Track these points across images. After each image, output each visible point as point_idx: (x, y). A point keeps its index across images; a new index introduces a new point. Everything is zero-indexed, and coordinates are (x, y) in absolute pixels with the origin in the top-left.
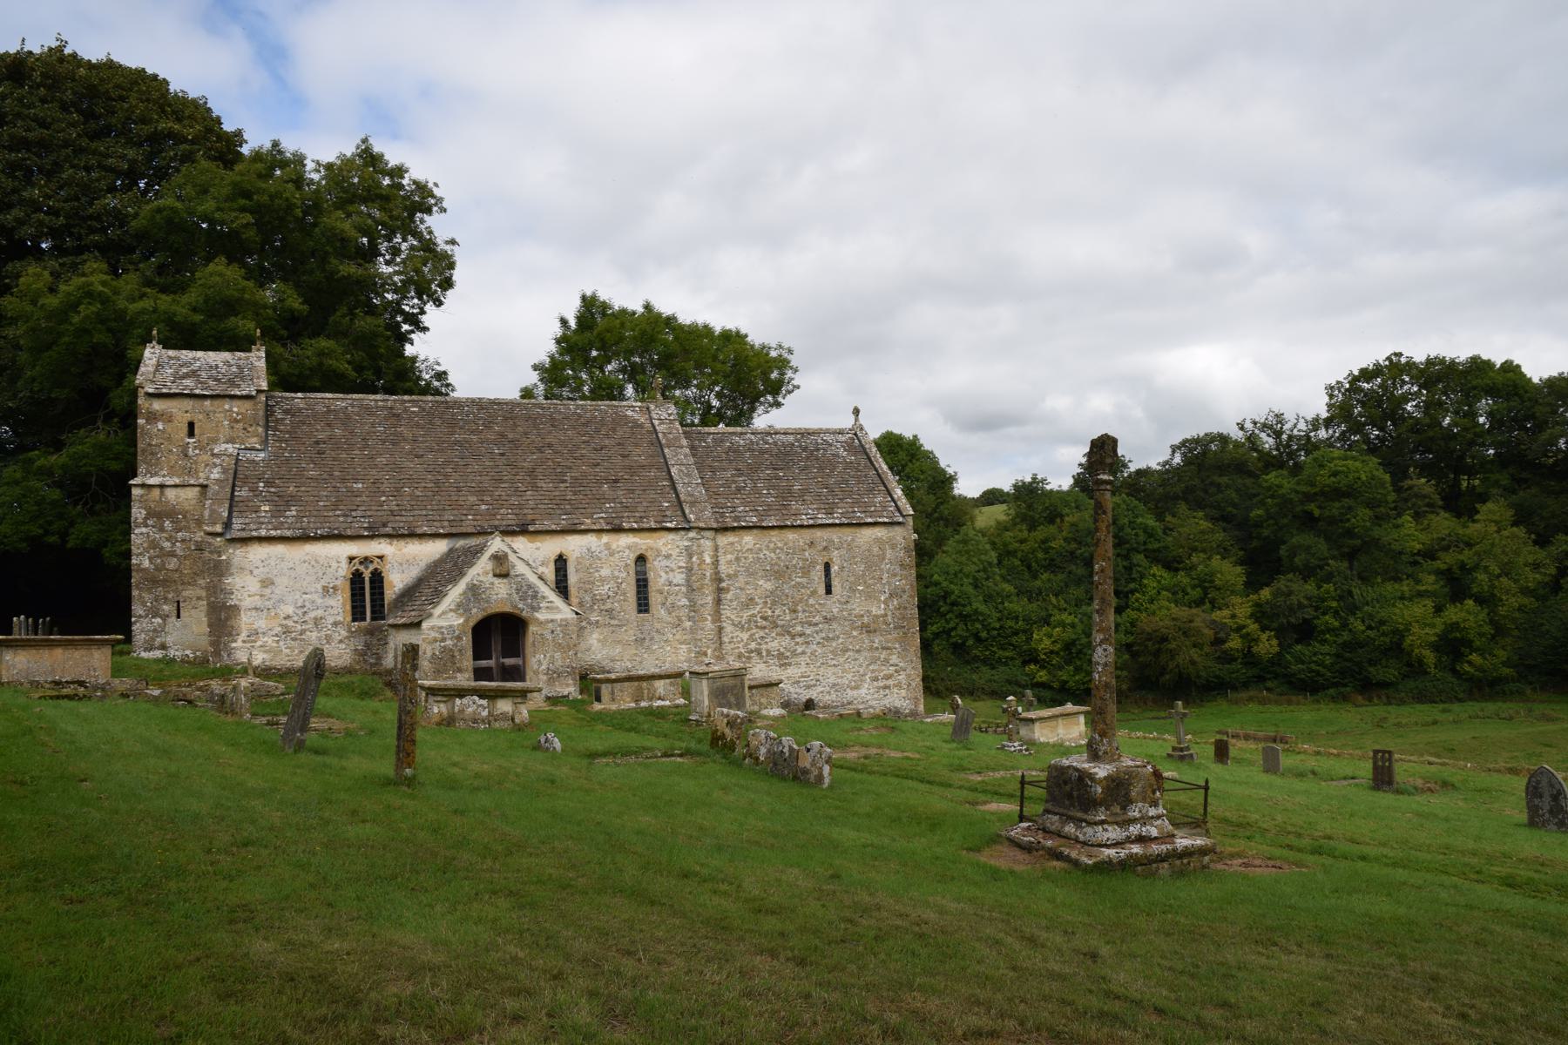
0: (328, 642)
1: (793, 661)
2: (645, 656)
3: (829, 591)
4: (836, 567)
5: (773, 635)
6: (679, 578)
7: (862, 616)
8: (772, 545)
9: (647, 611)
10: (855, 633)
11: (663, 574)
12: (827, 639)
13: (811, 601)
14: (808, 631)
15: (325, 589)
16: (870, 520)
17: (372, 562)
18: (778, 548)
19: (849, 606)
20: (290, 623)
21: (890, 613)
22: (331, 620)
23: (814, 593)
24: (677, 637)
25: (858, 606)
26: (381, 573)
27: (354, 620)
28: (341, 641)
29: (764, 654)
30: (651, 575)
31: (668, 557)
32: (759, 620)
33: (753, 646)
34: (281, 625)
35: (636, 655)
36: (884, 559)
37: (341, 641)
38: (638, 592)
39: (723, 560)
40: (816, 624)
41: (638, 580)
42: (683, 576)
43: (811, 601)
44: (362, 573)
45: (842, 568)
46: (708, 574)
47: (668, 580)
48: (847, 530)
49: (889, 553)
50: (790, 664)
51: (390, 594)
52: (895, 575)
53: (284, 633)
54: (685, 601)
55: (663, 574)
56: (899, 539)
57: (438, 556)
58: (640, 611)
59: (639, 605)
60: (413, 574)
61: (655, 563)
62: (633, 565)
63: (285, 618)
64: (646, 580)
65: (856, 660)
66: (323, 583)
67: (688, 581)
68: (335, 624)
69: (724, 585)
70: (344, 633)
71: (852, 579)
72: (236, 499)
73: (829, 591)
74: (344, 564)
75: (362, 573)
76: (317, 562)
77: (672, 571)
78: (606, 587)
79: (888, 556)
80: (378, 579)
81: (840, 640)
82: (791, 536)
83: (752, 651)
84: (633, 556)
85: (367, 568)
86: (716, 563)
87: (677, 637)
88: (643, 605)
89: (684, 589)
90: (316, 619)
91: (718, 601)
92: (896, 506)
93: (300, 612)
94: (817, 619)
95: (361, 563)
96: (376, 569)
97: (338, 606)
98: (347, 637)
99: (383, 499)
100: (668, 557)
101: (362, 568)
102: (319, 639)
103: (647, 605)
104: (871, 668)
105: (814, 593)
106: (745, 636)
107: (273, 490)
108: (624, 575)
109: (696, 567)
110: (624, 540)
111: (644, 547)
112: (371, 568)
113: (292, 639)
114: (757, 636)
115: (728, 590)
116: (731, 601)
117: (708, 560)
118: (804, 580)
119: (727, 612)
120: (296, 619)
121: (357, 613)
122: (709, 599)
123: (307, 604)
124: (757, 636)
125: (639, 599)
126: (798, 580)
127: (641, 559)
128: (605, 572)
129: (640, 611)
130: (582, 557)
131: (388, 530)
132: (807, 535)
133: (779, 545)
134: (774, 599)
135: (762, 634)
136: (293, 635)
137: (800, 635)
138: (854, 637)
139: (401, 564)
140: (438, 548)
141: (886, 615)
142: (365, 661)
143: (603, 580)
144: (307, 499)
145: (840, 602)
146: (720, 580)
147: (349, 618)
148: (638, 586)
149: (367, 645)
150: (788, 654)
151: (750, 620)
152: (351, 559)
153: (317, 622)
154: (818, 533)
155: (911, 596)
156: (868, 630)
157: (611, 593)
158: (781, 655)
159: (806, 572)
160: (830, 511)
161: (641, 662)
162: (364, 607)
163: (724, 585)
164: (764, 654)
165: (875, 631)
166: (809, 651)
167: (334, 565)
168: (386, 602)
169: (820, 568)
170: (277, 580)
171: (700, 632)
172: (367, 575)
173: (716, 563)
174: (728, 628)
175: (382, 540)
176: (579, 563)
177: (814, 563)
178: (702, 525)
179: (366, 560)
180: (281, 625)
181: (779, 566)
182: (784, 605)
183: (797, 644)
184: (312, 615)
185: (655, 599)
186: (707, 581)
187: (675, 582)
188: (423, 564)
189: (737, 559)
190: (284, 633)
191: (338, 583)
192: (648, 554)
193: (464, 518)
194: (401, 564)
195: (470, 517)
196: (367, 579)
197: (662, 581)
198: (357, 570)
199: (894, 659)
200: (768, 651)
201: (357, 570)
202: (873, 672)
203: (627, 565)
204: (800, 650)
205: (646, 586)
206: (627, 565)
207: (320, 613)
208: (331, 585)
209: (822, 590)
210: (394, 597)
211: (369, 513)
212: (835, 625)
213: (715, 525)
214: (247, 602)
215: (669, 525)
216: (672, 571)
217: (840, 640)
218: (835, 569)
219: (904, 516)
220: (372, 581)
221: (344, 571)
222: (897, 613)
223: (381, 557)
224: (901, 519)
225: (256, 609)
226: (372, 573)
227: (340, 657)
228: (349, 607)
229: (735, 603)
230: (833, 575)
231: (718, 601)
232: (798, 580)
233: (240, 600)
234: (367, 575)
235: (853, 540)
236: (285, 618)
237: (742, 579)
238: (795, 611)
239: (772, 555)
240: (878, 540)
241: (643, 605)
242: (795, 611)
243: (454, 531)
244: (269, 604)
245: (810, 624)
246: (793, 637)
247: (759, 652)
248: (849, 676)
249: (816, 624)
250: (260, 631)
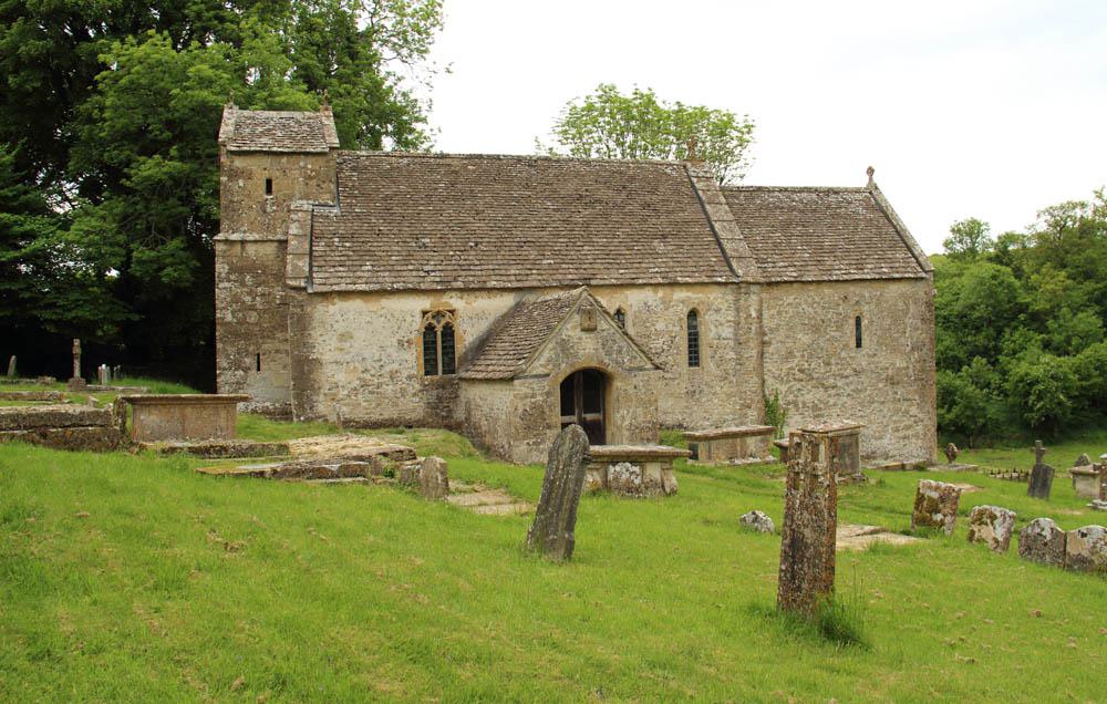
0: (403, 396)
1: (825, 412)
2: (696, 408)
3: (859, 345)
4: (866, 321)
5: (809, 387)
6: (727, 332)
7: (887, 369)
8: (810, 300)
9: (697, 364)
10: (881, 385)
11: (713, 328)
12: (857, 391)
13: (843, 354)
14: (839, 384)
15: (400, 343)
16: (897, 276)
17: (443, 316)
18: (815, 302)
19: (876, 359)
20: (367, 376)
21: (911, 366)
22: (405, 374)
23: (846, 346)
24: (725, 389)
25: (884, 359)
26: (451, 327)
27: (427, 373)
28: (415, 395)
29: (801, 406)
30: (702, 329)
31: (718, 311)
32: (797, 372)
33: (791, 398)
34: (359, 379)
35: (687, 407)
36: (907, 313)
37: (415, 395)
38: (690, 346)
39: (766, 314)
40: (847, 377)
41: (690, 334)
42: (731, 330)
43: (843, 354)
44: (434, 328)
45: (871, 322)
46: (753, 328)
47: (717, 333)
48: (876, 285)
49: (912, 307)
50: (822, 416)
51: (461, 348)
52: (918, 329)
53: (362, 386)
54: (732, 355)
55: (713, 328)
56: (921, 293)
57: (505, 310)
58: (690, 365)
59: (690, 358)
60: (482, 327)
61: (707, 317)
62: (686, 319)
63: (363, 372)
64: (696, 334)
65: (881, 411)
66: (398, 337)
67: (736, 335)
68: (410, 377)
69: (766, 338)
70: (418, 387)
71: (879, 333)
72: (315, 253)
73: (859, 345)
74: (418, 318)
75: (434, 328)
76: (392, 315)
77: (721, 324)
78: (661, 341)
79: (911, 310)
80: (449, 332)
81: (868, 392)
82: (827, 291)
83: (789, 403)
84: (686, 311)
85: (439, 322)
86: (760, 317)
87: (725, 389)
88: (694, 359)
89: (732, 343)
90: (391, 372)
91: (762, 355)
92: (918, 262)
93: (377, 365)
94: (849, 372)
95: (433, 317)
96: (448, 323)
97: (413, 359)
98: (420, 391)
99: (451, 253)
100: (718, 311)
101: (434, 322)
102: (395, 391)
103: (697, 358)
104: (894, 418)
105: (846, 346)
106: (784, 388)
107: (347, 244)
108: (678, 328)
109: (743, 321)
110: (680, 294)
111: (696, 301)
112: (443, 322)
113: (370, 392)
114: (794, 388)
115: (770, 343)
116: (772, 354)
117: (754, 314)
118: (837, 334)
119: (768, 366)
120: (372, 372)
121: (430, 367)
122: (754, 352)
123: (383, 358)
124: (794, 388)
125: (690, 353)
126: (833, 333)
127: (693, 314)
128: (660, 326)
129: (690, 365)
130: (640, 312)
131: (459, 284)
132: (842, 290)
133: (817, 299)
134: (811, 352)
135: (799, 386)
136: (370, 388)
137: (833, 387)
138: (880, 389)
139: (471, 318)
140: (506, 302)
141: (908, 367)
142: (437, 414)
143: (658, 334)
144: (380, 253)
145: (869, 356)
146: (764, 334)
147: (423, 372)
148: (690, 340)
149: (439, 398)
150: (822, 406)
151: (788, 374)
152: (425, 313)
153: (393, 375)
154: (851, 288)
155: (929, 350)
156: (892, 381)
157: (665, 347)
158: (815, 407)
159: (839, 327)
160: (860, 266)
161: (691, 414)
162: (436, 360)
163: (766, 338)
164: (801, 406)
165: (898, 383)
166: (840, 402)
167: (409, 319)
168: (457, 356)
169: (852, 322)
170: (356, 334)
171: (746, 384)
172: (439, 329)
173: (760, 317)
174: (769, 381)
175: (453, 294)
176: (636, 317)
177: (846, 317)
178: (750, 279)
179: (438, 315)
180: (359, 379)
181: (816, 320)
182: (819, 358)
183: (830, 396)
184: (388, 369)
185: (705, 352)
186: (752, 335)
187: (724, 335)
188: (492, 319)
189: (779, 313)
190: (362, 386)
191: (412, 336)
192: (700, 308)
193: (529, 272)
194: (471, 318)
195: (534, 272)
196: (439, 333)
197: (712, 335)
198: (430, 324)
199: (914, 410)
200: (804, 403)
201: (430, 324)
202: (895, 422)
203: (681, 319)
204: (832, 402)
205: (696, 340)
206: (681, 319)
207: (395, 366)
208: (406, 339)
209: (853, 343)
210: (464, 350)
211: (440, 267)
212: (863, 378)
213: (762, 280)
214: (327, 357)
215: (719, 279)
216: (721, 324)
217: (868, 392)
218: (865, 323)
219: (926, 272)
220: (443, 334)
221: (418, 324)
222: (918, 366)
223: (452, 312)
224: (924, 275)
225: (337, 362)
226: (444, 327)
227: (414, 410)
228: (422, 361)
229: (776, 356)
230: (863, 328)
231: (762, 355)
232: (833, 333)
233: (322, 354)
234: (439, 329)
235: (881, 294)
236: (363, 372)
237: (782, 332)
238: (829, 364)
239: (810, 309)
240: (902, 295)
241: (694, 359)
242: (829, 364)
243: (520, 285)
244: (348, 358)
245: (842, 377)
246: (826, 389)
247: (795, 404)
248: (874, 427)
249: (847, 377)
250: (340, 384)
